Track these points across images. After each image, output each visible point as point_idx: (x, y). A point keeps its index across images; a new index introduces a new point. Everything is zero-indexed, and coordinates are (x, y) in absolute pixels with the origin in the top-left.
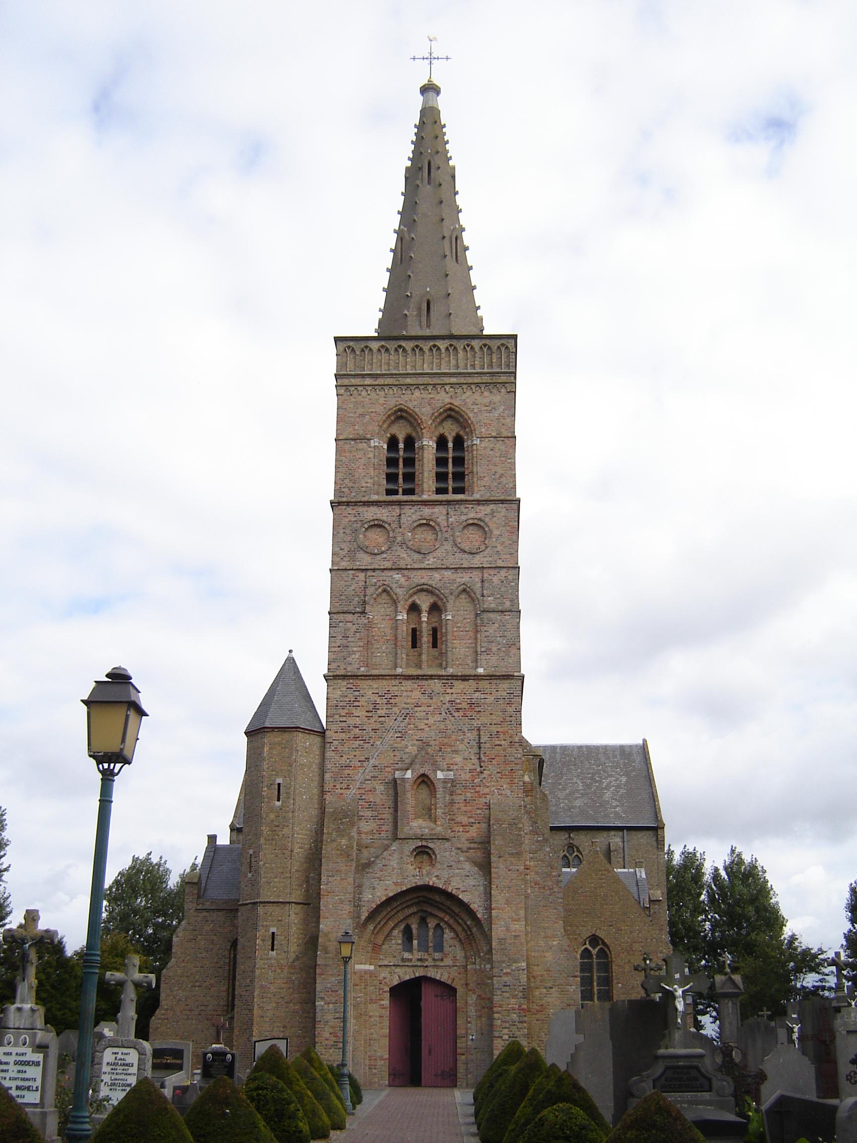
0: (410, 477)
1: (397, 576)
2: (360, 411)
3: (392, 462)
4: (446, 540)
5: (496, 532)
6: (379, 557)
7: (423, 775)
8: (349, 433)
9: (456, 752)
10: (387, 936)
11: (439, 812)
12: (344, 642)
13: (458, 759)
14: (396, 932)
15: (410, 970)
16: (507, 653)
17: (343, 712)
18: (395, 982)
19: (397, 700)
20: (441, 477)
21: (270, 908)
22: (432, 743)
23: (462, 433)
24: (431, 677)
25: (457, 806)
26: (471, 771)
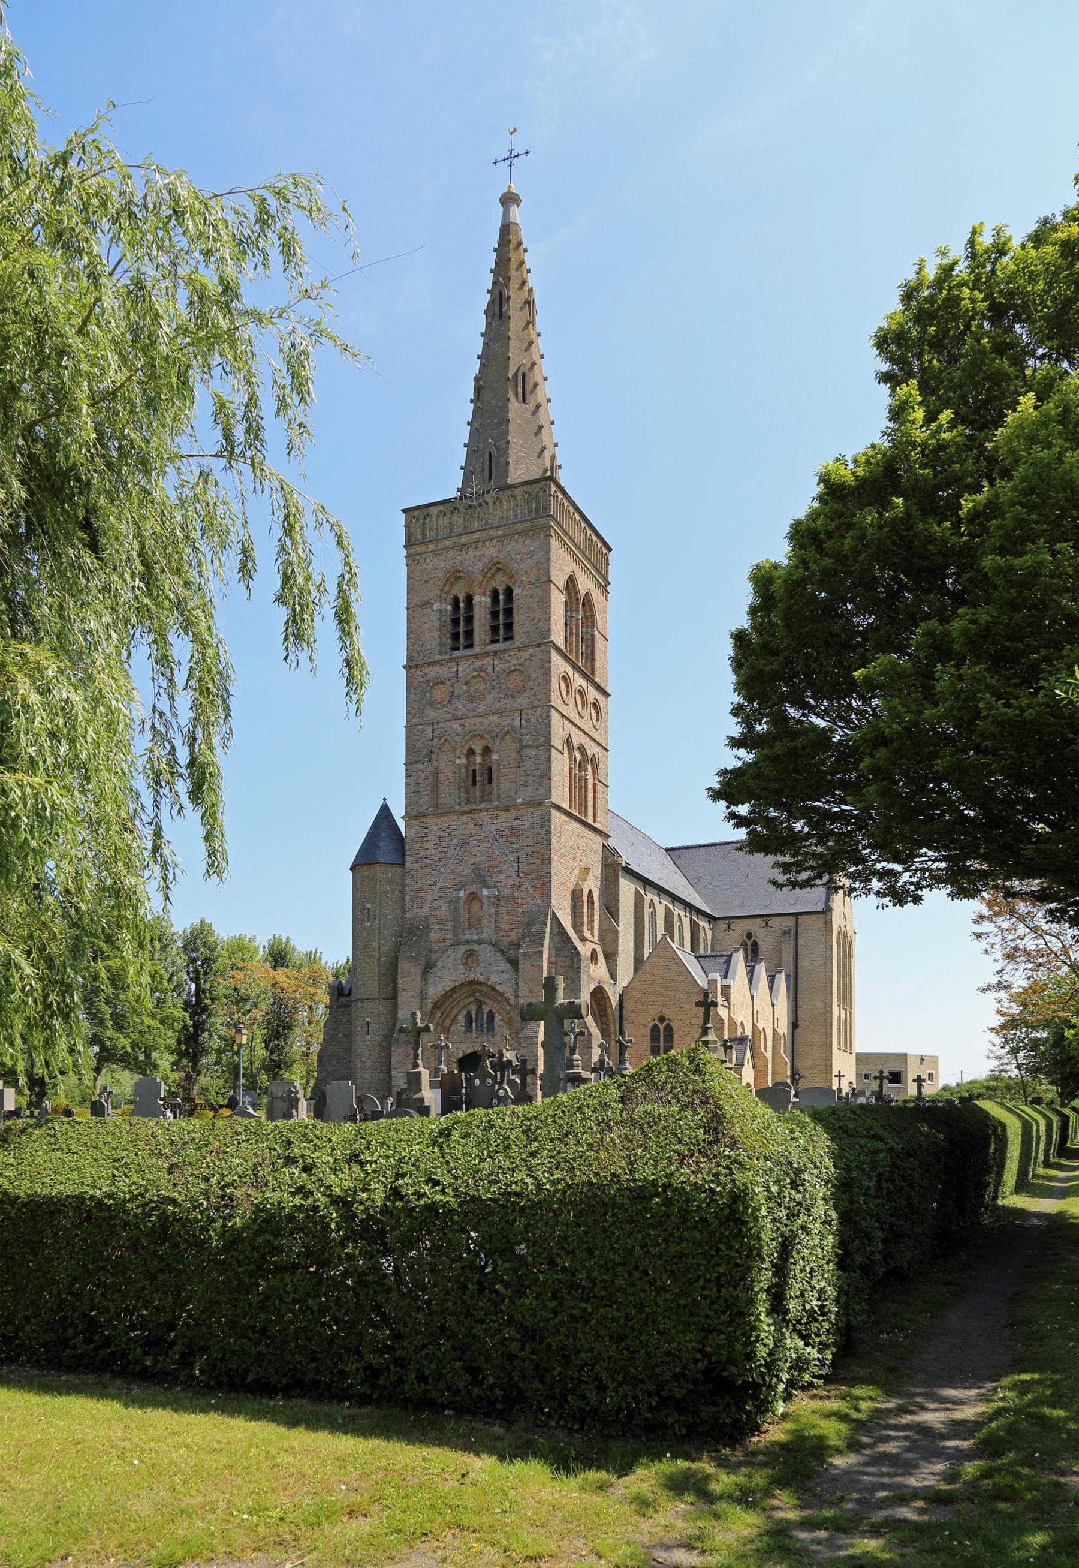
0: (469, 634)
1: (456, 726)
2: (425, 578)
3: (455, 622)
4: (493, 688)
5: (534, 675)
6: (441, 711)
7: (473, 893)
8: (417, 600)
9: (500, 871)
10: (453, 1021)
11: (485, 921)
12: (417, 788)
13: (502, 877)
14: (460, 1017)
15: (470, 1045)
16: (540, 784)
17: (416, 846)
18: (461, 1055)
19: (456, 832)
20: (495, 629)
21: (366, 1003)
22: (483, 866)
23: (510, 584)
24: (481, 811)
25: (501, 916)
26: (512, 886)
